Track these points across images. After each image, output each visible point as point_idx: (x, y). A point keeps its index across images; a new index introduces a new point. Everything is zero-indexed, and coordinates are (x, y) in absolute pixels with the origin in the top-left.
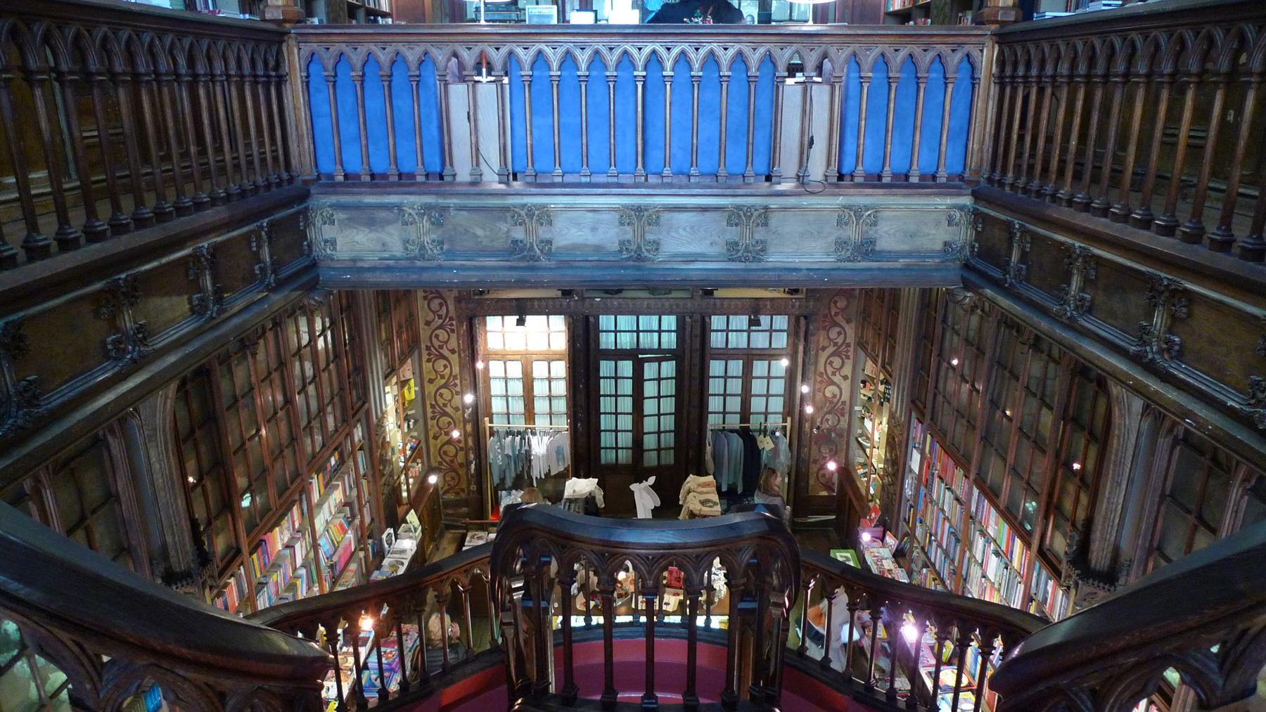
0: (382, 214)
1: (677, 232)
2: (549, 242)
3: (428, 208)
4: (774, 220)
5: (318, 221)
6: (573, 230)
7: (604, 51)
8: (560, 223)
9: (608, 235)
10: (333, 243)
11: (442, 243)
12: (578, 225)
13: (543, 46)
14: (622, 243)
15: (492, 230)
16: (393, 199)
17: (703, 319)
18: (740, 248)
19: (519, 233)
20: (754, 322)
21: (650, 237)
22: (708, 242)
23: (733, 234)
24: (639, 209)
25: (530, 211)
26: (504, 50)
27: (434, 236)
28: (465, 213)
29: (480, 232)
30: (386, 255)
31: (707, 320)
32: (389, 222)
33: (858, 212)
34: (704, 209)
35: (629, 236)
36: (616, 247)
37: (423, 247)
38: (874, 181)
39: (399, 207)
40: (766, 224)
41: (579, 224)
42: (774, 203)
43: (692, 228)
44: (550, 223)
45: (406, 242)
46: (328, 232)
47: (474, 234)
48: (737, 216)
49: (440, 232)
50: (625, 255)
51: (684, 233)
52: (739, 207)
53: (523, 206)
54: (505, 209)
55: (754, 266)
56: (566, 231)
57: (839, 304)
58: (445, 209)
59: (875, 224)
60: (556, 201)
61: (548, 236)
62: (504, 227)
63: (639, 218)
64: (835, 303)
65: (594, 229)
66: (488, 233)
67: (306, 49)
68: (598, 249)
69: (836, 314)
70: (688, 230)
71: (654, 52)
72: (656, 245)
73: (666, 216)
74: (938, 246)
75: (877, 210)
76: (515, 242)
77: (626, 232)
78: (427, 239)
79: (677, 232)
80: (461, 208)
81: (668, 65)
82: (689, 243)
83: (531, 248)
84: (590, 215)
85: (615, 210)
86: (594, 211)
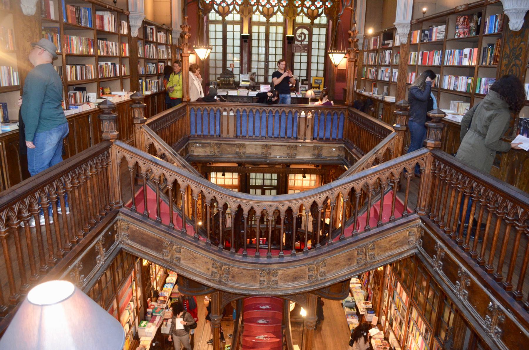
0: (206, 145)
2: (245, 152)
3: (217, 144)
4: (298, 149)
5: (190, 146)
7: (259, 110)
8: (247, 148)
9: (259, 151)
10: (193, 151)
11: (219, 152)
12: (252, 148)
13: (246, 108)
14: (262, 153)
16: (208, 141)
17: (286, 175)
19: (238, 150)
20: (304, 177)
21: (269, 152)
23: (288, 151)
24: (266, 145)
25: (241, 145)
26: (236, 109)
27: (217, 150)
29: (228, 149)
30: (206, 154)
31: (287, 175)
32: (207, 147)
33: (318, 147)
36: (261, 154)
37: (215, 153)
38: (321, 139)
39: (210, 143)
40: (296, 149)
42: (298, 144)
44: (245, 148)
45: (211, 152)
46: (193, 149)
48: (289, 147)
50: (263, 156)
52: (290, 145)
53: (239, 144)
54: (235, 144)
55: (293, 159)
57: (333, 171)
58: (221, 144)
59: (322, 150)
60: (247, 143)
61: (244, 151)
62: (234, 148)
63: (266, 147)
64: (331, 171)
65: (255, 149)
67: (191, 107)
68: (256, 154)
69: (332, 175)
71: (271, 110)
72: (270, 154)
73: (273, 147)
74: (337, 155)
75: (322, 147)
76: (237, 152)
78: (216, 151)
80: (224, 144)
81: (274, 113)
85: (261, 145)
86: (256, 145)
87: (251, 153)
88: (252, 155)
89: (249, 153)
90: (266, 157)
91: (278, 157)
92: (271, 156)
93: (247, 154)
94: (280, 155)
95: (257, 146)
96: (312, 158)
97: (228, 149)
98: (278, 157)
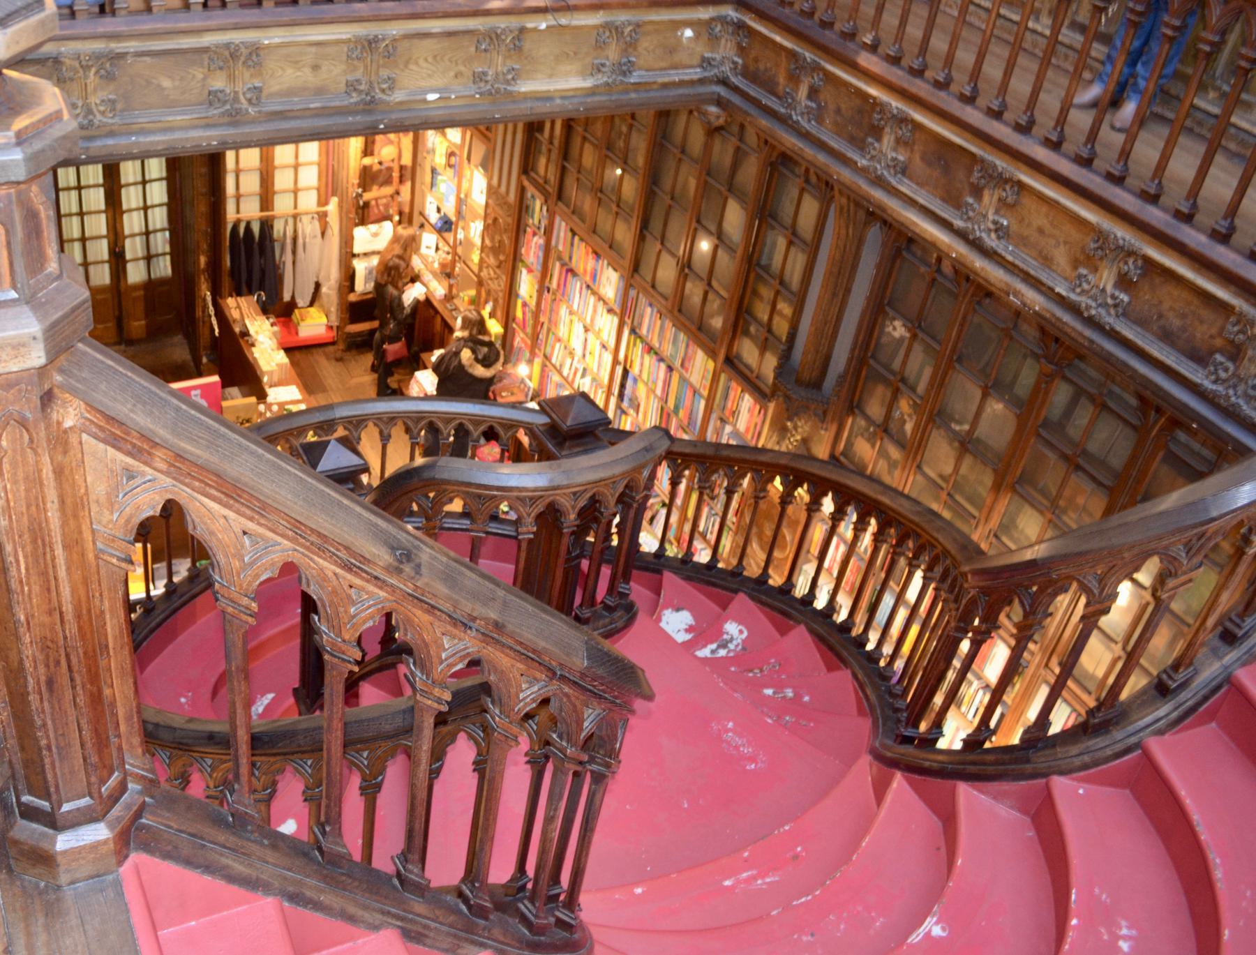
1: (417, 63)
2: (258, 90)
6: (289, 71)
8: (271, 64)
11: (113, 102)
12: (296, 63)
15: (182, 79)
18: (489, 78)
19: (219, 82)
22: (452, 74)
24: (371, 43)
28: (147, 59)
29: (166, 83)
34: (450, 34)
35: (359, 74)
36: (342, 87)
37: (89, 112)
41: (297, 62)
43: (435, 57)
47: (159, 86)
49: (112, 87)
50: (355, 98)
51: (425, 65)
54: (205, 50)
56: (280, 72)
58: (122, 56)
62: (199, 73)
65: (316, 68)
66: (177, 83)
68: (320, 91)
70: (430, 59)
77: (355, 69)
78: (94, 100)
79: (417, 63)
82: (429, 76)
83: (236, 100)
84: (313, 49)
87: (290, 92)
88: (297, 103)
89: (281, 94)
90: (370, 105)
91: (432, 97)
92: (398, 96)
93: (270, 95)
94: (439, 82)
95: (329, 50)
96: (588, 83)
97: (166, 83)
98: (432, 97)
